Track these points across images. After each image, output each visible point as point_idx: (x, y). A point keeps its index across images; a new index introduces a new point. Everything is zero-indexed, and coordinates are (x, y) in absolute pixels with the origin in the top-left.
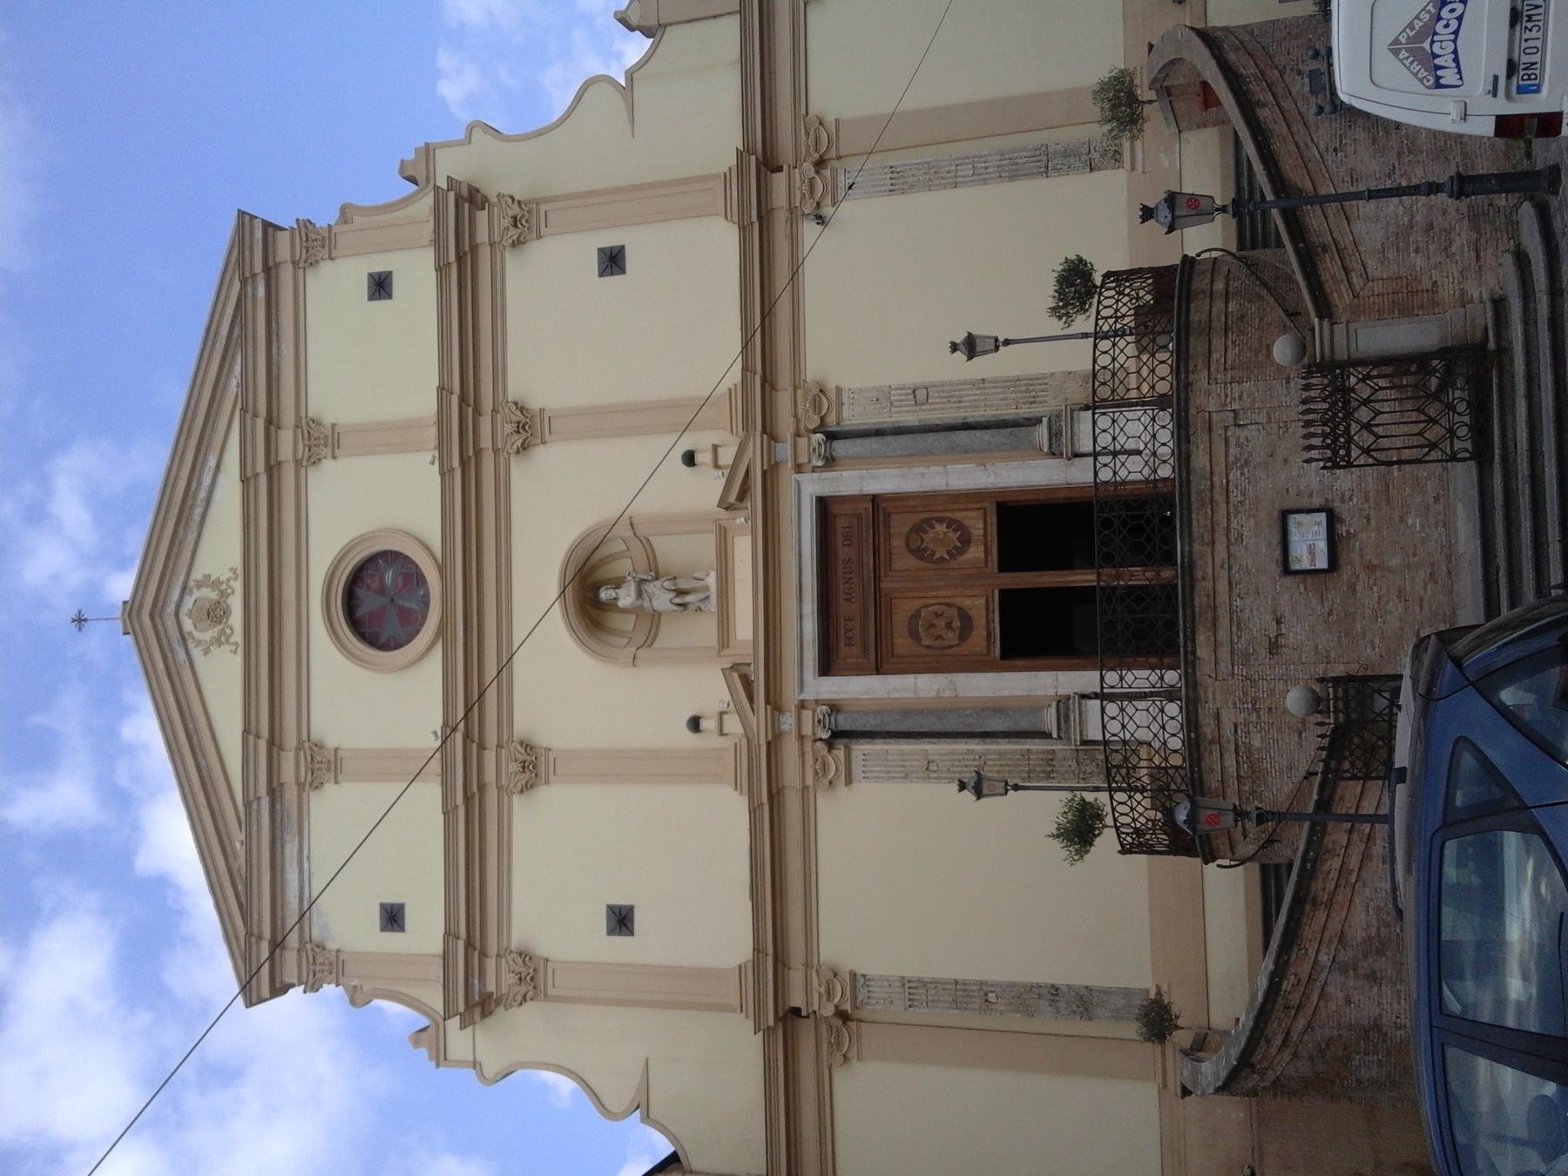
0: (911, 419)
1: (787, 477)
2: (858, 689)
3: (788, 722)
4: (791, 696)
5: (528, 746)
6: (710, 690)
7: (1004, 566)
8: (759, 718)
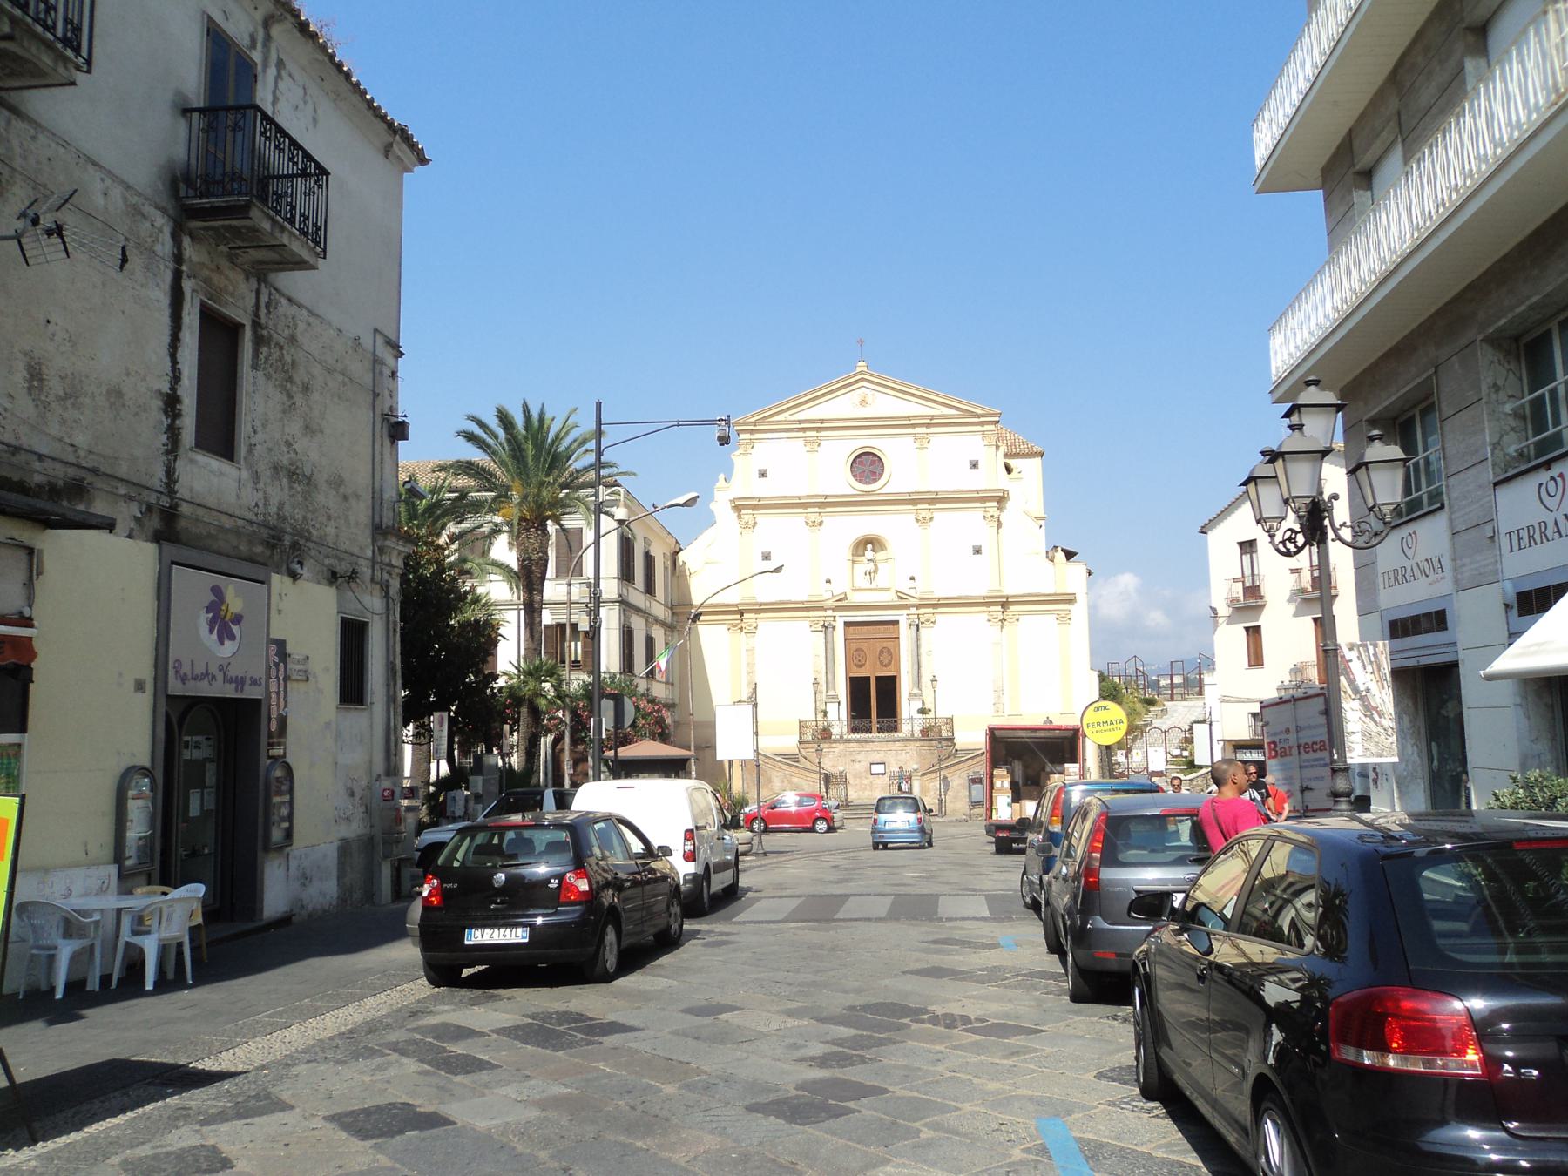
0: (922, 650)
1: (905, 612)
2: (839, 636)
3: (830, 613)
4: (837, 614)
5: (821, 523)
6: (839, 588)
7: (878, 678)
8: (831, 603)
